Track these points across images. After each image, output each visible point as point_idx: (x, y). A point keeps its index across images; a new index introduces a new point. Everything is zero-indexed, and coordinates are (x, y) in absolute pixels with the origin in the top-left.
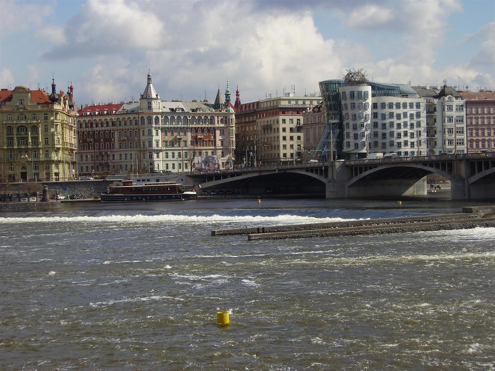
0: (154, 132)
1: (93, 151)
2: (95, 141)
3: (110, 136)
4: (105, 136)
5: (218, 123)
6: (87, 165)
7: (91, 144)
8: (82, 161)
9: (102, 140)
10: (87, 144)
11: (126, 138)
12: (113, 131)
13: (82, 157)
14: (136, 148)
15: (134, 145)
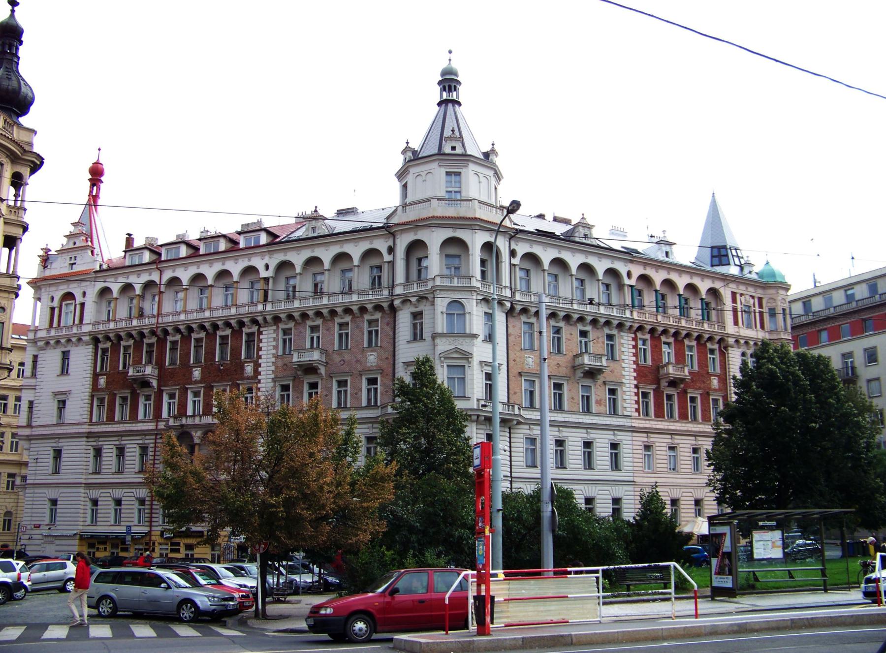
0: (476, 323)
1: (151, 426)
2: (164, 376)
3: (236, 352)
4: (211, 353)
5: (736, 323)
6: (118, 493)
7: (147, 391)
8: (97, 472)
9: (197, 374)
10: (127, 393)
11: (316, 356)
12: (255, 329)
13: (98, 452)
14: (369, 406)
15: (357, 394)
